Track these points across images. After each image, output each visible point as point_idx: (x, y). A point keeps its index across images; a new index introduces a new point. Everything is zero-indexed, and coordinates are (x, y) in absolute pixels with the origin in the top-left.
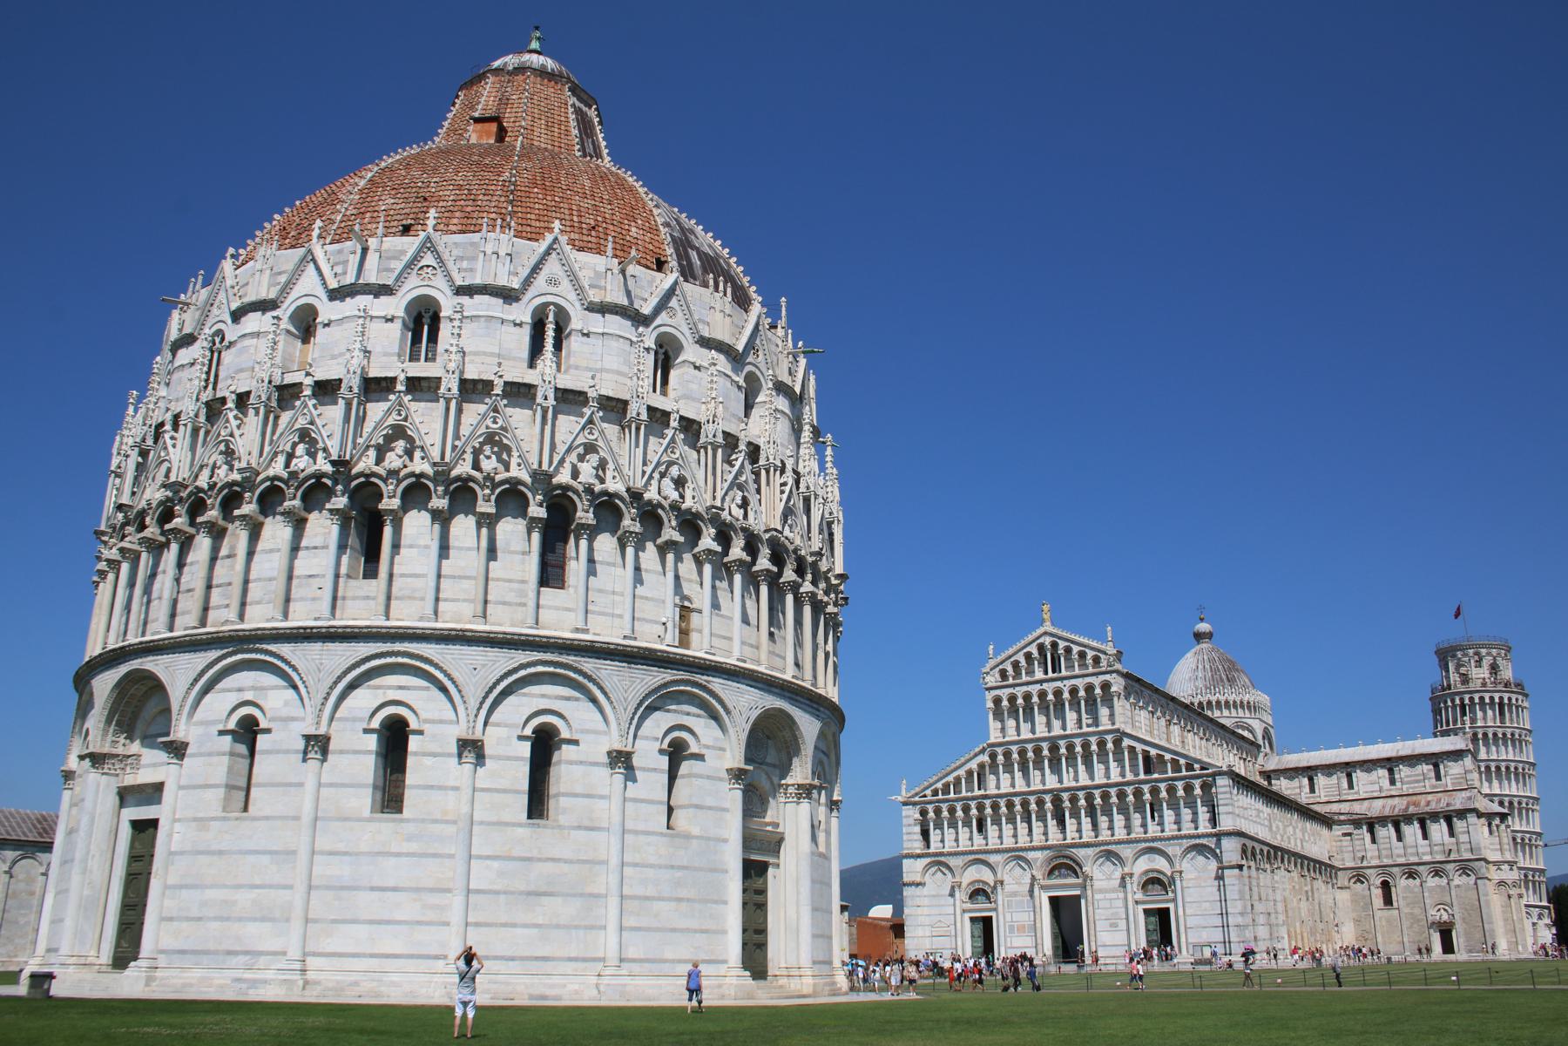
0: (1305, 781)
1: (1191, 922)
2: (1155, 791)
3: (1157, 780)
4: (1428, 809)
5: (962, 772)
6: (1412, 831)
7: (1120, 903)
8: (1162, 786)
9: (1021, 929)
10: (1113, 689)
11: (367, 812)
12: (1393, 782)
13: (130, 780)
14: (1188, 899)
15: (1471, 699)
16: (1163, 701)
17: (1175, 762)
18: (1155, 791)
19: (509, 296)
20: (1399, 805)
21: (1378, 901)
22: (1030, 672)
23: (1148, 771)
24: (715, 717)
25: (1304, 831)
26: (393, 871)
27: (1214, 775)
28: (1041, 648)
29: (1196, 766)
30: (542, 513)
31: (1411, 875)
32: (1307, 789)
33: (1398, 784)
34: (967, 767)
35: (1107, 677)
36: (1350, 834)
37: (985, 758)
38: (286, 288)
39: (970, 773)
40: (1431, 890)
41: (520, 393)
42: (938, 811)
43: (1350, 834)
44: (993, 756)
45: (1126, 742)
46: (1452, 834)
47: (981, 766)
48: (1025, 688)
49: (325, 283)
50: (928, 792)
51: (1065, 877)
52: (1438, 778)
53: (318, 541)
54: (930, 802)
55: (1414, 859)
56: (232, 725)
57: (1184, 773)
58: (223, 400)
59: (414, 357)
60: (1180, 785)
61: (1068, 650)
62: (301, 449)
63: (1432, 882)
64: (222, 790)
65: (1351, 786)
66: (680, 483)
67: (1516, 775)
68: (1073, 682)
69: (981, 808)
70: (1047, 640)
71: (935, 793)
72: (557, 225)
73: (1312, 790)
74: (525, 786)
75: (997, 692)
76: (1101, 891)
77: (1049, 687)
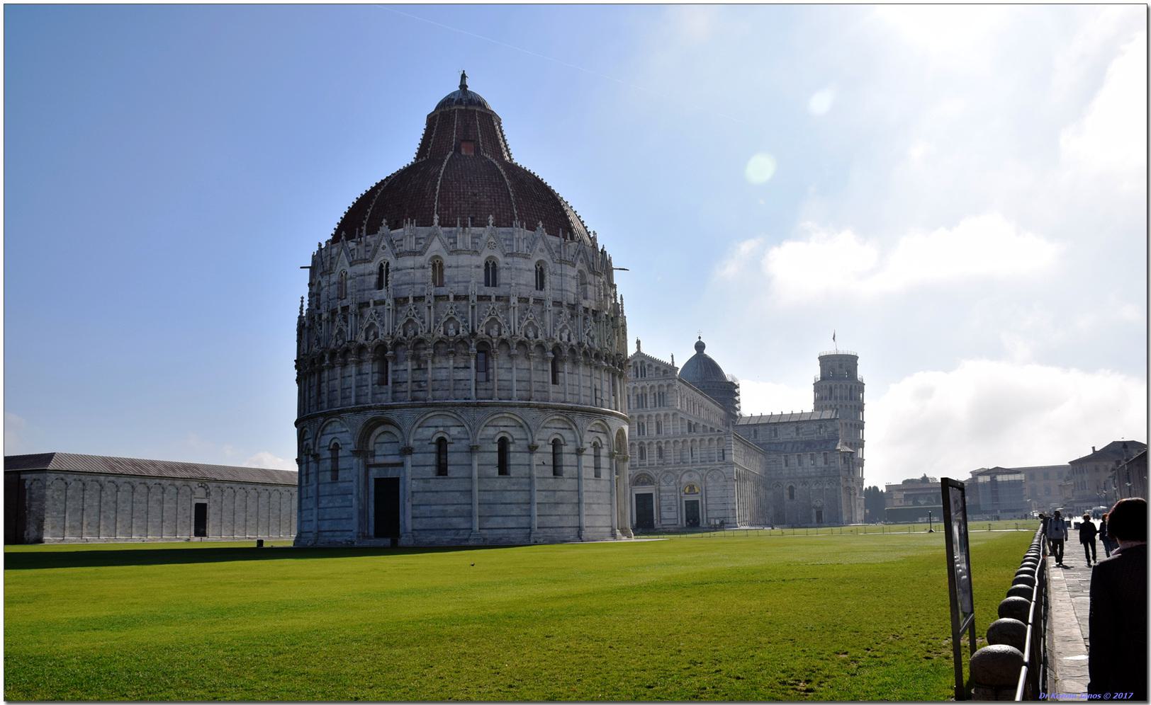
1: (710, 507)
11: (497, 475)
13: (371, 461)
19: (526, 257)
21: (787, 497)
24: (605, 433)
26: (509, 497)
30: (550, 355)
38: (426, 247)
41: (539, 301)
45: (681, 415)
49: (445, 247)
53: (462, 365)
56: (434, 440)
58: (406, 299)
59: (487, 284)
62: (451, 326)
63: (814, 488)
64: (434, 468)
66: (593, 339)
70: (638, 360)
72: (541, 224)
74: (551, 462)
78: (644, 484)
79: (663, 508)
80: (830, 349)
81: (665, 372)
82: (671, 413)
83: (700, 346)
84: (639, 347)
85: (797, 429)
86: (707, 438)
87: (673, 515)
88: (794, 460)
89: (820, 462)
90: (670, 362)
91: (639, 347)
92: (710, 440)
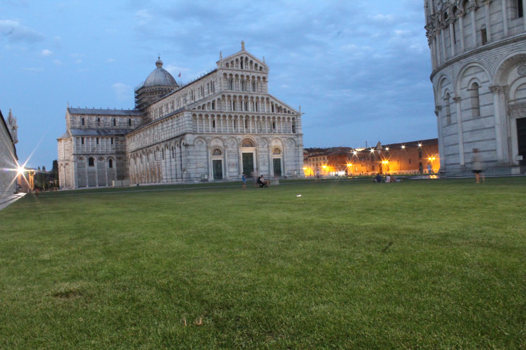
9: (233, 165)
28: (242, 58)
29: (292, 112)
35: (265, 75)
70: (244, 56)
76: (260, 152)
77: (240, 73)
84: (243, 47)
91: (243, 47)
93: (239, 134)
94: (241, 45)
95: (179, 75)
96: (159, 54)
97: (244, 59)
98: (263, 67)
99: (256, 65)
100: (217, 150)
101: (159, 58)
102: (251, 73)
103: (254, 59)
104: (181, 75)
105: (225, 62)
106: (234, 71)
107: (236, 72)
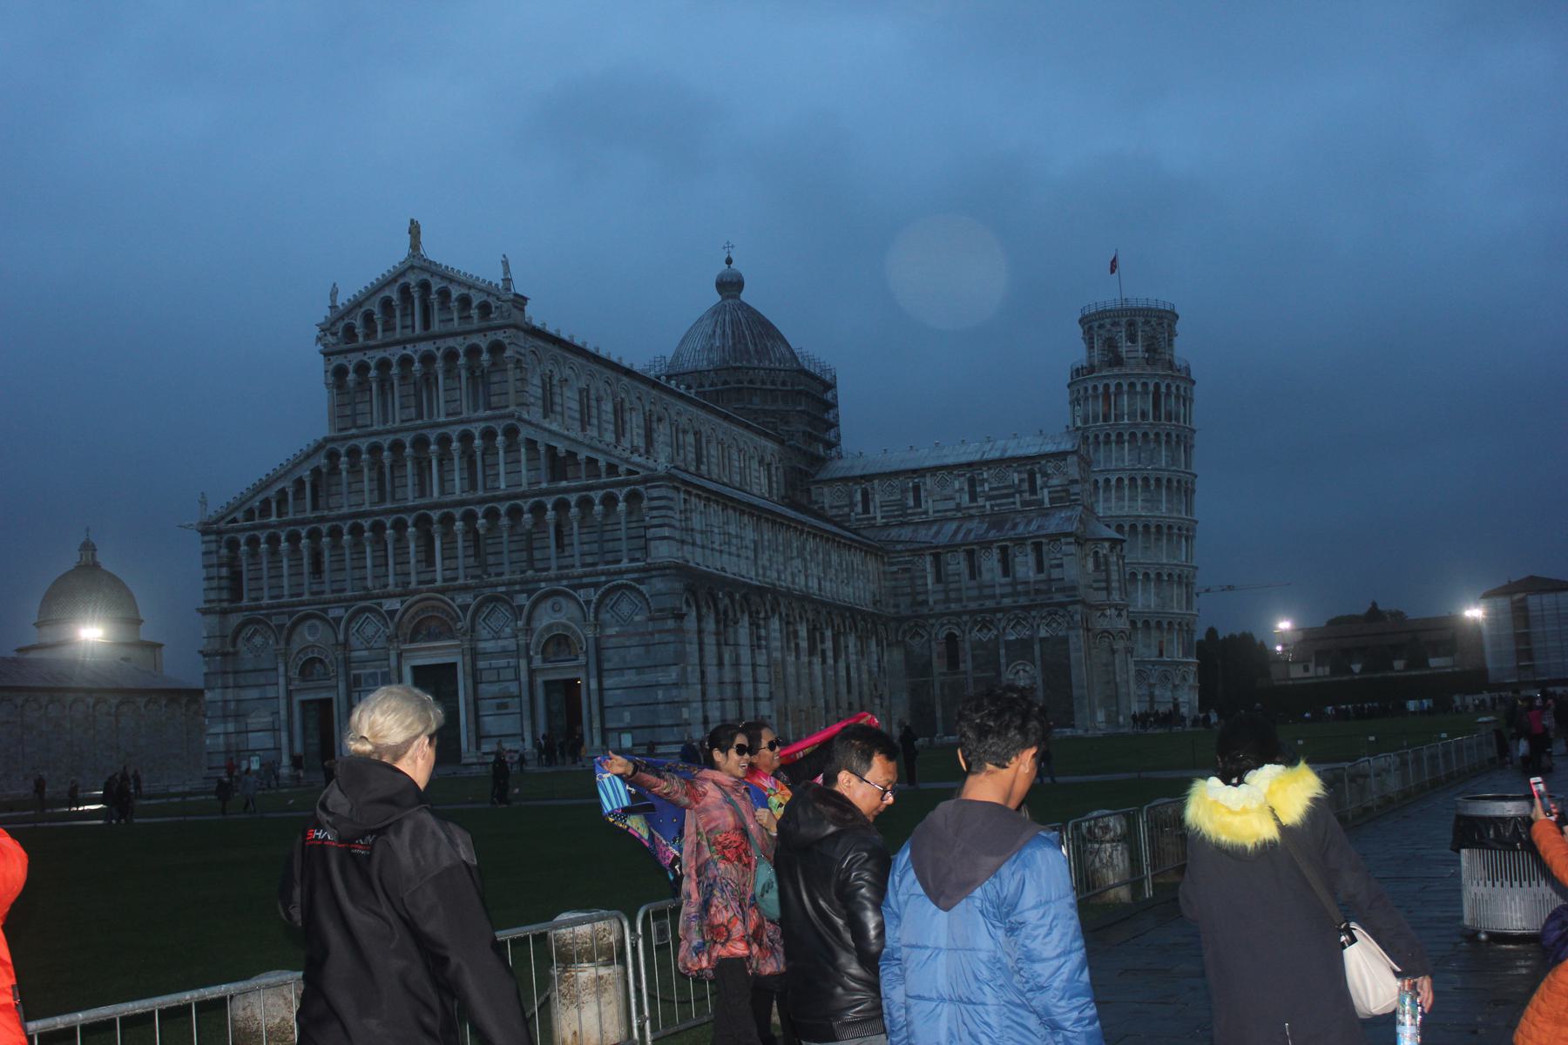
0: (858, 497)
1: (612, 697)
2: (562, 506)
3: (566, 490)
4: (1011, 534)
5: (287, 484)
6: (990, 564)
7: (510, 674)
8: (573, 498)
10: (509, 353)
12: (973, 498)
14: (606, 666)
15: (1119, 385)
16: (609, 373)
17: (591, 462)
18: (562, 506)
20: (977, 528)
22: (389, 327)
23: (553, 479)
25: (827, 565)
27: (645, 481)
28: (405, 291)
29: (622, 468)
31: (985, 625)
32: (859, 508)
33: (981, 501)
34: (296, 474)
36: (908, 570)
37: (321, 461)
39: (300, 483)
40: (1008, 644)
42: (253, 542)
43: (908, 570)
44: (333, 456)
45: (525, 432)
46: (1040, 568)
47: (316, 472)
48: (380, 354)
50: (239, 515)
51: (437, 637)
52: (1033, 490)
54: (245, 530)
55: (990, 604)
57: (604, 480)
60: (597, 496)
61: (445, 294)
65: (918, 502)
67: (1169, 487)
68: (451, 342)
69: (314, 535)
70: (412, 279)
71: (250, 514)
73: (866, 510)
75: (337, 360)
78: (432, 636)
79: (487, 707)
80: (1106, 295)
81: (485, 309)
82: (499, 426)
83: (730, 286)
84: (415, 244)
85: (972, 483)
86: (597, 496)
87: (507, 724)
88: (957, 564)
89: (1025, 567)
90: (496, 278)
91: (415, 244)
92: (609, 501)
93: (390, 596)
94: (407, 239)
95: (1114, 266)
96: (729, 246)
97: (416, 294)
98: (491, 300)
99: (465, 302)
100: (312, 661)
101: (729, 261)
102: (439, 343)
103: (451, 280)
104: (1120, 262)
105: (341, 325)
106: (370, 353)
107: (380, 354)
